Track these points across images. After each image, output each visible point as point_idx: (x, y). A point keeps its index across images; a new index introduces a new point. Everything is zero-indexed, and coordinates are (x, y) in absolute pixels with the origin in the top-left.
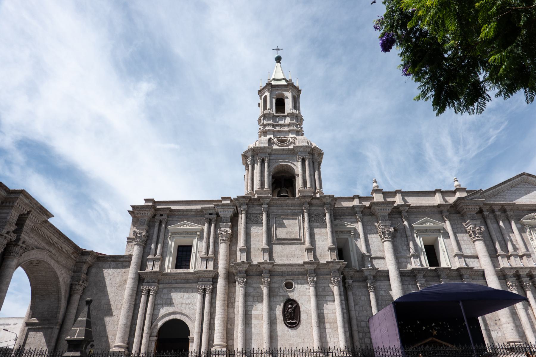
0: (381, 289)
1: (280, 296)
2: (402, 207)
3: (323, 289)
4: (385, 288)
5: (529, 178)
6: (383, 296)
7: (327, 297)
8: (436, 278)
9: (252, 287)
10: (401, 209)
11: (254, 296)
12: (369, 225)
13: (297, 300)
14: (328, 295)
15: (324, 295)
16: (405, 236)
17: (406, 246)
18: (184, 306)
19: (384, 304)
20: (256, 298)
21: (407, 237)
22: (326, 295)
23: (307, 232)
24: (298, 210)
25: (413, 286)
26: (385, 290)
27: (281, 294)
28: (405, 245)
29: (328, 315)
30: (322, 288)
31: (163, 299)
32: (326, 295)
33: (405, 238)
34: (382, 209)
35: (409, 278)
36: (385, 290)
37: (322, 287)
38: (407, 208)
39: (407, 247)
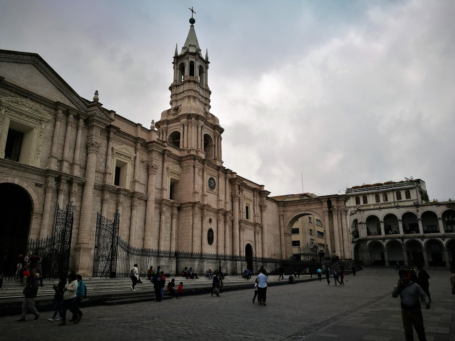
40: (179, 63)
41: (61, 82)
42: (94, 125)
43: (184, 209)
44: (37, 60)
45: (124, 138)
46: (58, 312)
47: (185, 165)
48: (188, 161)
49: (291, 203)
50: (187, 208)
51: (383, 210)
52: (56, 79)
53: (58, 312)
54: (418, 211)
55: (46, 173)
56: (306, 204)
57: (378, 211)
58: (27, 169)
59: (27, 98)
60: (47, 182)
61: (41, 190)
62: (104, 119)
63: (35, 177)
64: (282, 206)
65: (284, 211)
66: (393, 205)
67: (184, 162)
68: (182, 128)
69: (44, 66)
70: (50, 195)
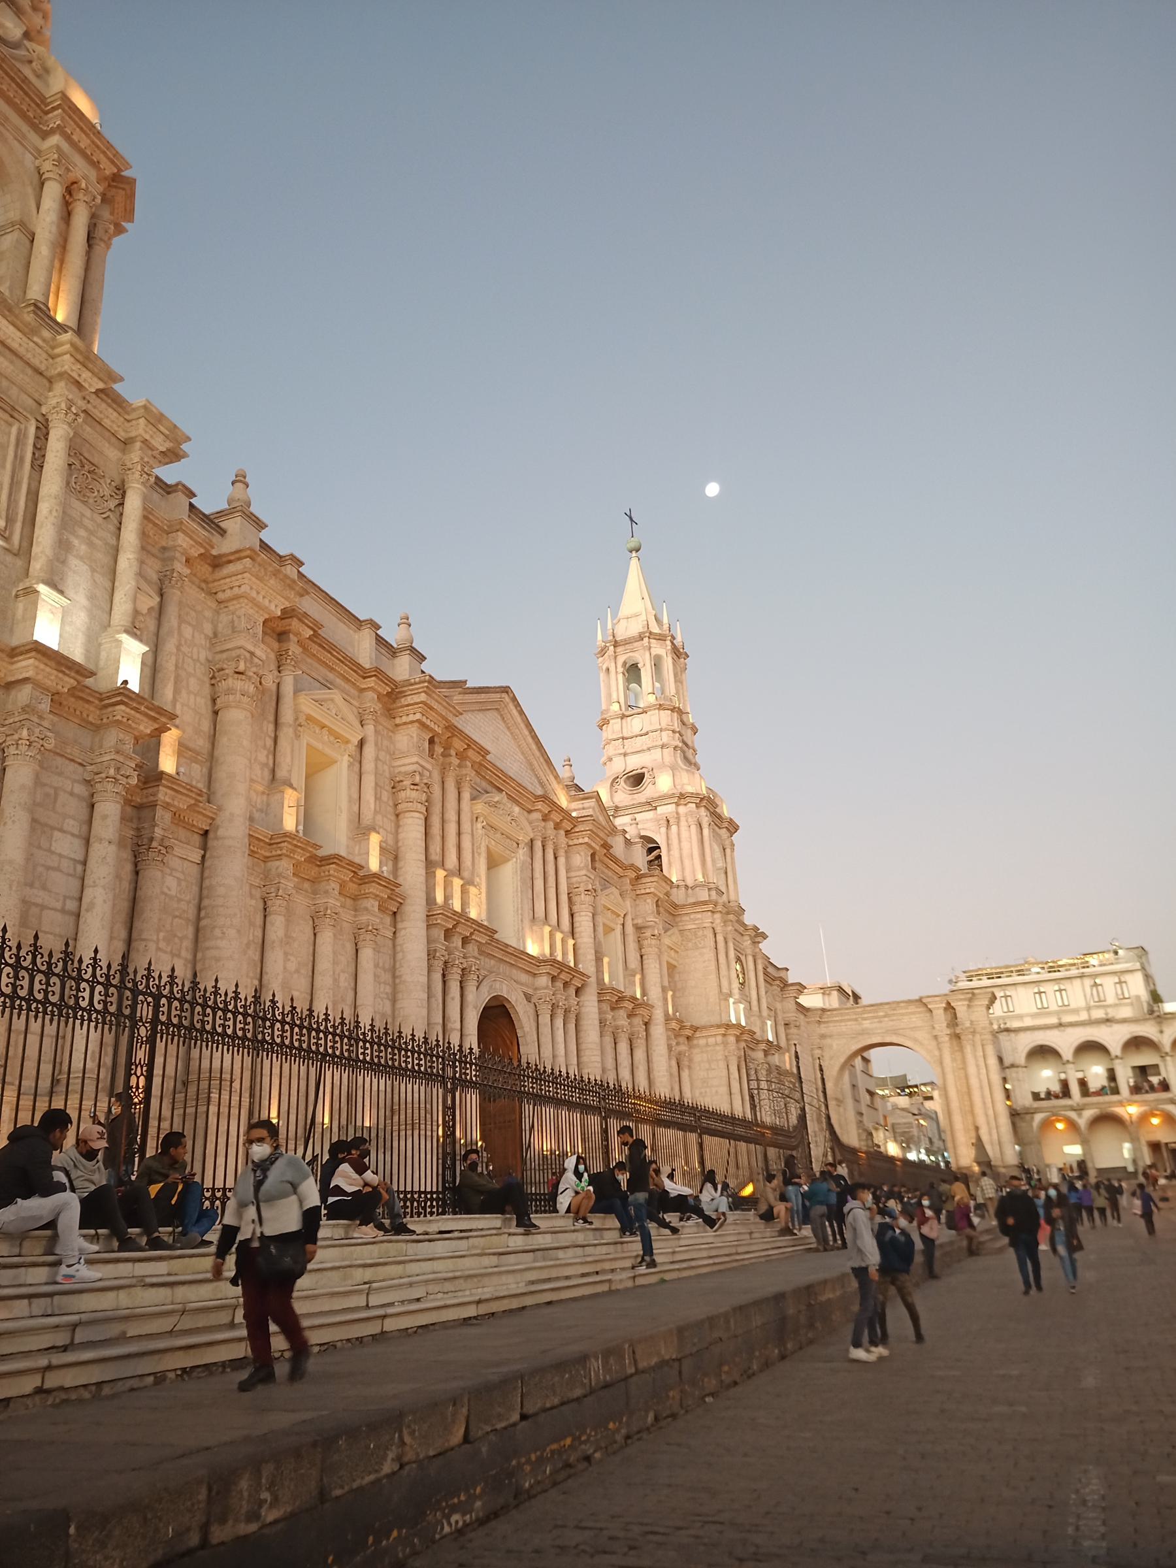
0: (172, 869)
2: (300, 620)
3: (47, 795)
4: (183, 872)
5: (511, 706)
6: (171, 898)
7: (57, 834)
10: (292, 627)
12: (189, 624)
14: (61, 830)
15: (46, 825)
17: (265, 752)
19: (168, 927)
22: (53, 828)
23: (52, 519)
24: (22, 390)
25: (254, 892)
26: (182, 877)
28: (265, 747)
29: (46, 912)
30: (47, 789)
32: (53, 828)
33: (271, 727)
34: (263, 593)
36: (182, 877)
37: (45, 785)
38: (308, 630)
39: (267, 757)
40: (621, 660)
41: (534, 747)
43: (702, 1042)
46: (273, 1328)
47: (689, 927)
48: (699, 916)
50: (711, 1040)
51: (1070, 1030)
53: (273, 1328)
54: (1161, 1032)
56: (885, 1016)
57: (1055, 1032)
61: (530, 1009)
66: (1084, 1016)
67: (686, 918)
68: (663, 830)
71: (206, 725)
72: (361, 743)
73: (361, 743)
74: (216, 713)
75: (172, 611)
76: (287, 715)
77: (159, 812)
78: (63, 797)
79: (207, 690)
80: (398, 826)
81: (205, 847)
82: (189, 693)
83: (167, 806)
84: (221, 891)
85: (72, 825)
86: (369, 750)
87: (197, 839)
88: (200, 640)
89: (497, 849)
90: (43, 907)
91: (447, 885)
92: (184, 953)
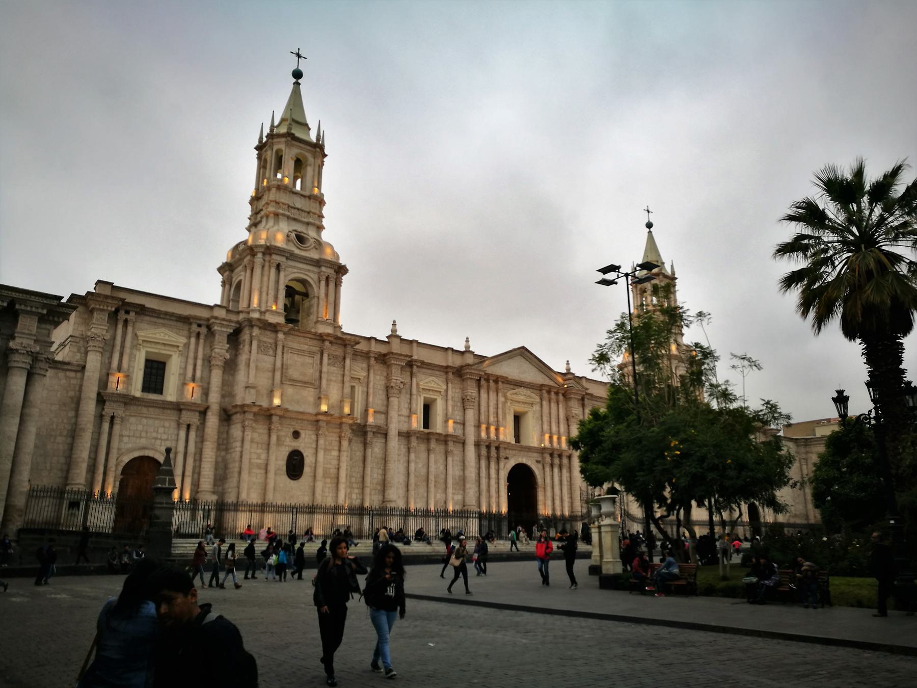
1: (286, 446)
8: (426, 441)
9: (256, 432)
11: (258, 443)
13: (302, 451)
16: (409, 393)
18: (158, 442)
20: (260, 445)
21: (411, 394)
22: (331, 450)
27: (286, 443)
31: (130, 430)
33: (409, 396)
35: (403, 438)
42: (571, 398)
44: (524, 350)
45: (596, 401)
49: (817, 441)
52: (538, 362)
55: (542, 451)
58: (529, 449)
59: (521, 386)
60: (544, 458)
61: (540, 466)
62: (580, 391)
63: (535, 455)
64: (803, 445)
65: (807, 453)
69: (529, 354)
70: (548, 469)
71: (385, 403)
72: (447, 391)
73: (447, 391)
74: (388, 398)
75: (372, 375)
76: (414, 391)
77: (369, 433)
78: (333, 442)
79: (385, 393)
80: (464, 413)
81: (386, 438)
82: (379, 394)
83: (371, 431)
84: (389, 450)
85: (337, 448)
86: (450, 392)
87: (383, 436)
88: (382, 378)
89: (520, 408)
90: (330, 469)
91: (488, 429)
92: (382, 468)
